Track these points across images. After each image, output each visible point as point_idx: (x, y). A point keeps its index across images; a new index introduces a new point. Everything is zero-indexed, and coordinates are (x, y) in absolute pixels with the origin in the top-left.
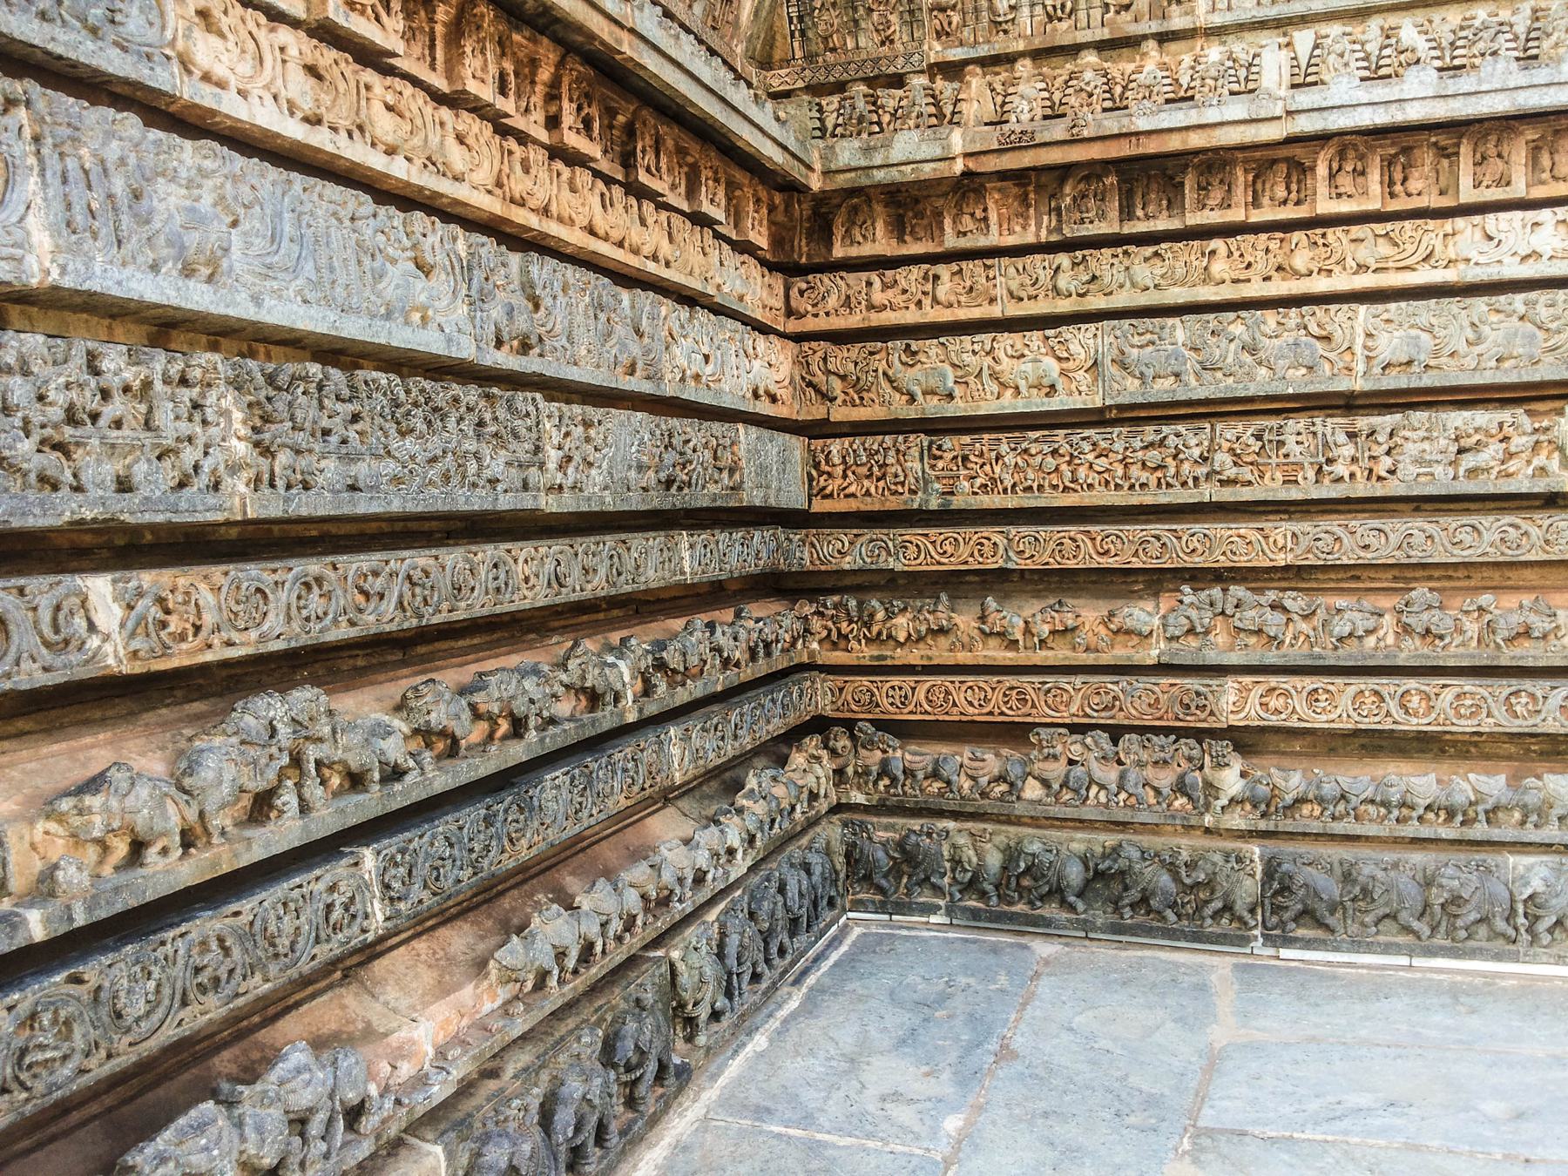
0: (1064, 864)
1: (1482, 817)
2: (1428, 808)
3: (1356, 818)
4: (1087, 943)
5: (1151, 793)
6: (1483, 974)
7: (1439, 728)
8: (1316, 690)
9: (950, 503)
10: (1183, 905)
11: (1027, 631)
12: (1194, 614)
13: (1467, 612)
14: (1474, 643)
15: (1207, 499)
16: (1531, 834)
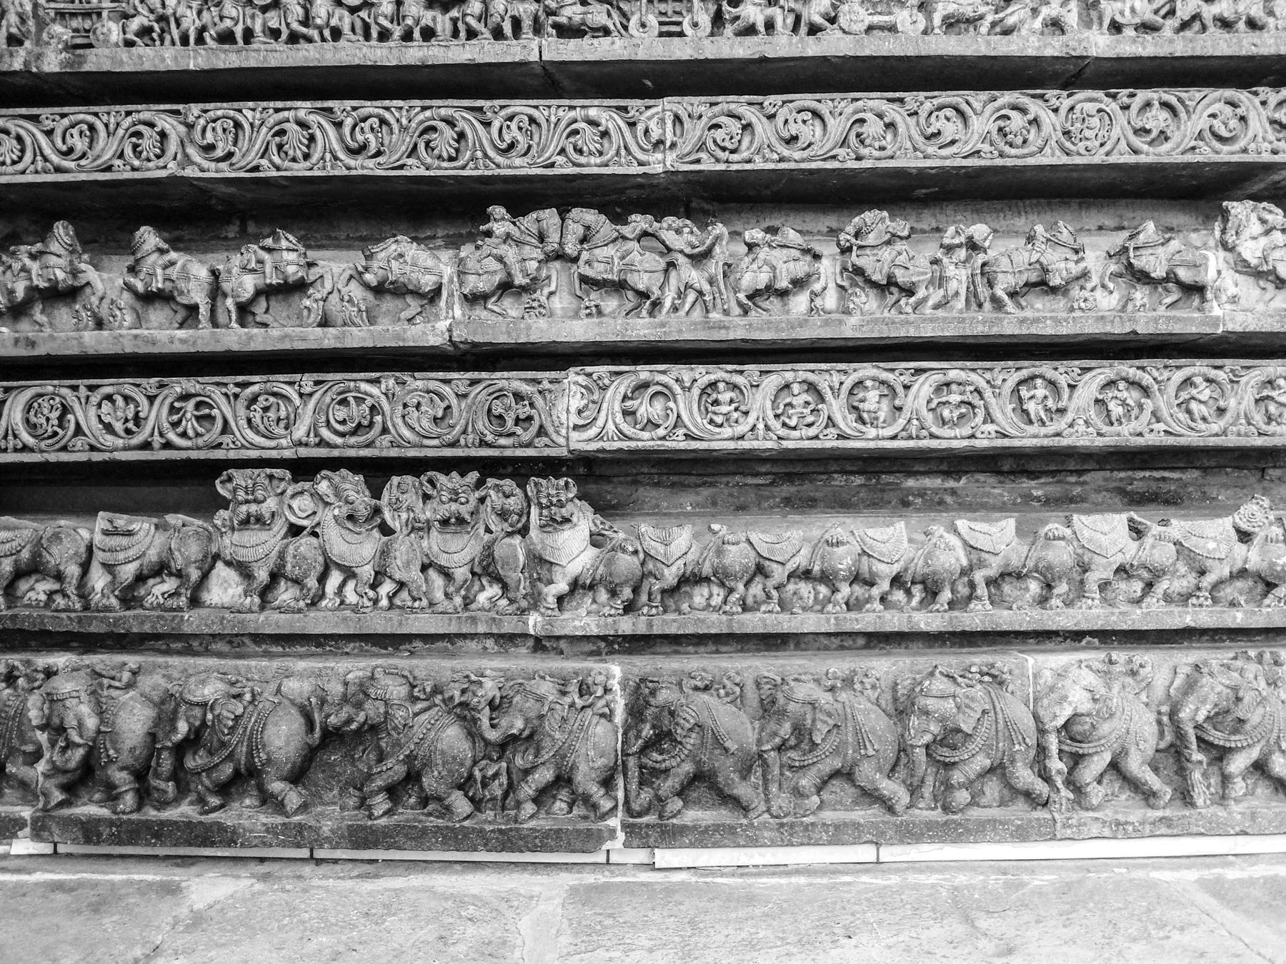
0: (263, 725)
1: (982, 590)
2: (897, 581)
3: (782, 604)
4: (307, 869)
5: (438, 581)
6: (1000, 867)
7: (911, 444)
8: (713, 385)
9: (82, 60)
10: (485, 785)
11: (216, 292)
12: (510, 253)
13: (949, 249)
14: (960, 303)
15: (534, 57)
16: (1061, 617)
